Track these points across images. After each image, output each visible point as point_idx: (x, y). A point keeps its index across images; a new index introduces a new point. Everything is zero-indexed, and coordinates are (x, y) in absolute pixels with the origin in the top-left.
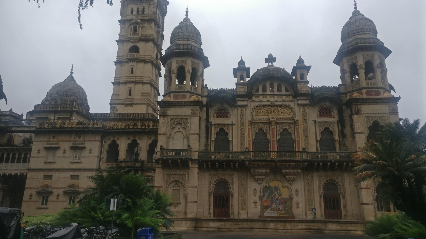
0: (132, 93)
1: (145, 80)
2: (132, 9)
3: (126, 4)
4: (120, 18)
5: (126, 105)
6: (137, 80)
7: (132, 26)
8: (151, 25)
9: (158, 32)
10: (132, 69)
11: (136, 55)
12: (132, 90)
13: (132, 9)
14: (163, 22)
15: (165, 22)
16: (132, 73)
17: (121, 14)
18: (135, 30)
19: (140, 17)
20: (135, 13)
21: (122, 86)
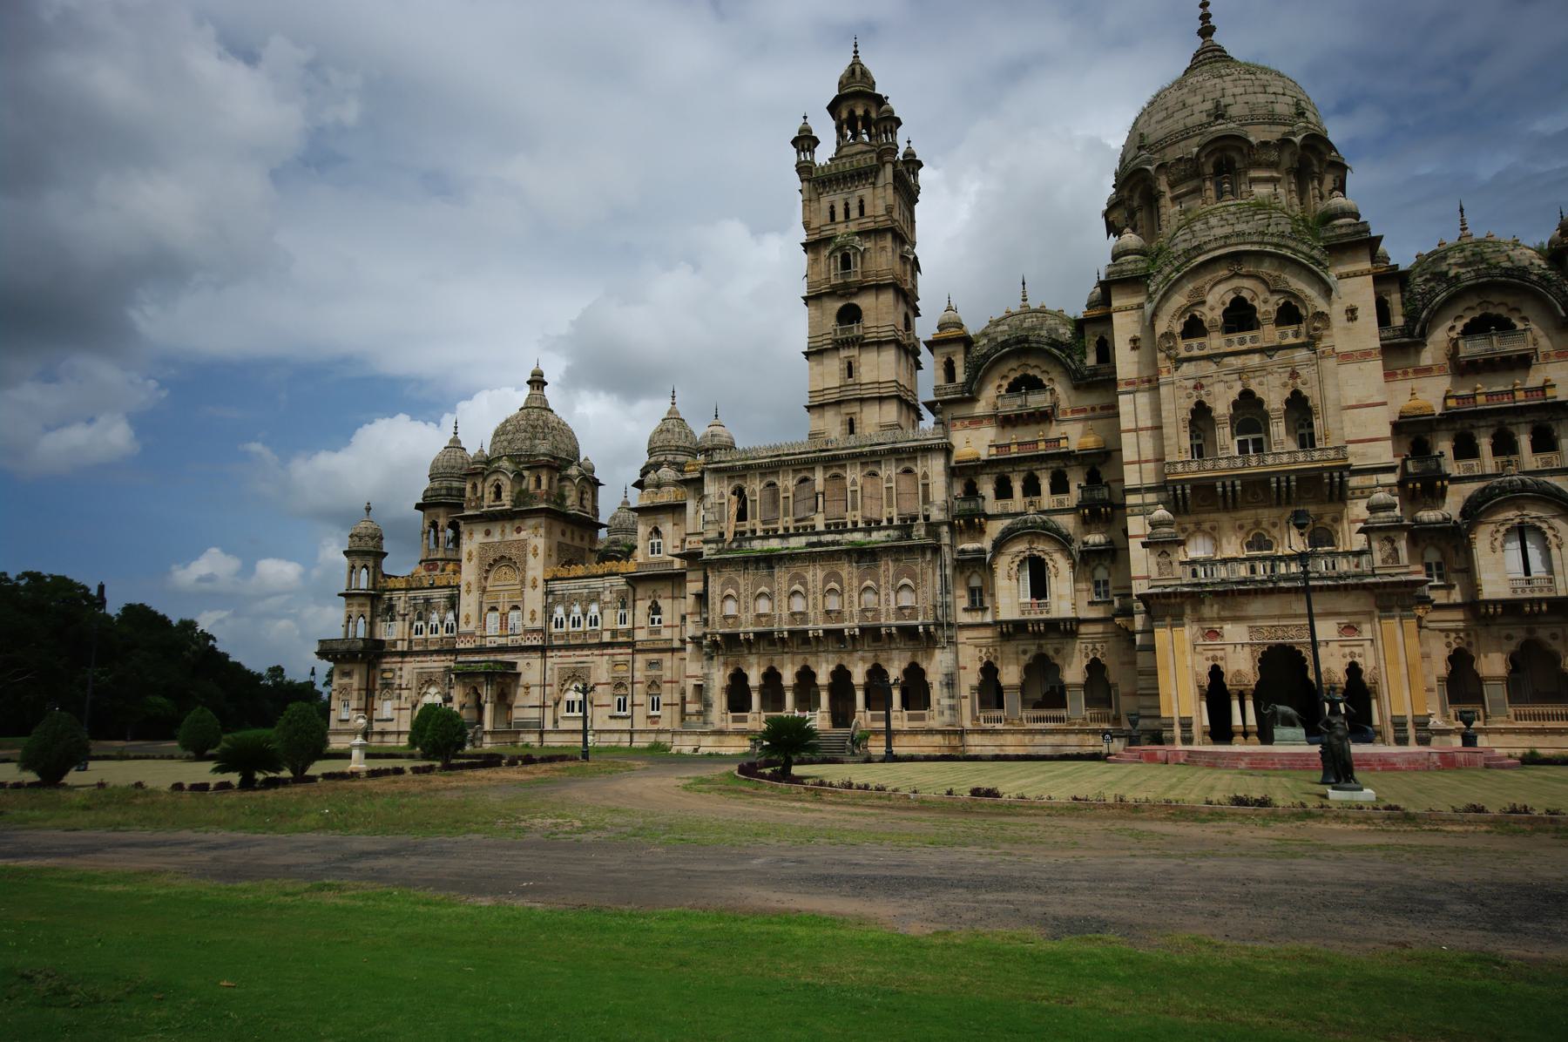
0: (857, 430)
1: (884, 392)
2: (832, 207)
3: (814, 196)
4: (803, 237)
6: (866, 394)
7: (839, 255)
8: (881, 244)
9: (904, 258)
10: (850, 364)
11: (857, 331)
12: (857, 418)
13: (832, 207)
14: (913, 222)
15: (917, 218)
16: (850, 376)
17: (806, 225)
18: (846, 263)
19: (853, 227)
20: (840, 216)
21: (830, 414)
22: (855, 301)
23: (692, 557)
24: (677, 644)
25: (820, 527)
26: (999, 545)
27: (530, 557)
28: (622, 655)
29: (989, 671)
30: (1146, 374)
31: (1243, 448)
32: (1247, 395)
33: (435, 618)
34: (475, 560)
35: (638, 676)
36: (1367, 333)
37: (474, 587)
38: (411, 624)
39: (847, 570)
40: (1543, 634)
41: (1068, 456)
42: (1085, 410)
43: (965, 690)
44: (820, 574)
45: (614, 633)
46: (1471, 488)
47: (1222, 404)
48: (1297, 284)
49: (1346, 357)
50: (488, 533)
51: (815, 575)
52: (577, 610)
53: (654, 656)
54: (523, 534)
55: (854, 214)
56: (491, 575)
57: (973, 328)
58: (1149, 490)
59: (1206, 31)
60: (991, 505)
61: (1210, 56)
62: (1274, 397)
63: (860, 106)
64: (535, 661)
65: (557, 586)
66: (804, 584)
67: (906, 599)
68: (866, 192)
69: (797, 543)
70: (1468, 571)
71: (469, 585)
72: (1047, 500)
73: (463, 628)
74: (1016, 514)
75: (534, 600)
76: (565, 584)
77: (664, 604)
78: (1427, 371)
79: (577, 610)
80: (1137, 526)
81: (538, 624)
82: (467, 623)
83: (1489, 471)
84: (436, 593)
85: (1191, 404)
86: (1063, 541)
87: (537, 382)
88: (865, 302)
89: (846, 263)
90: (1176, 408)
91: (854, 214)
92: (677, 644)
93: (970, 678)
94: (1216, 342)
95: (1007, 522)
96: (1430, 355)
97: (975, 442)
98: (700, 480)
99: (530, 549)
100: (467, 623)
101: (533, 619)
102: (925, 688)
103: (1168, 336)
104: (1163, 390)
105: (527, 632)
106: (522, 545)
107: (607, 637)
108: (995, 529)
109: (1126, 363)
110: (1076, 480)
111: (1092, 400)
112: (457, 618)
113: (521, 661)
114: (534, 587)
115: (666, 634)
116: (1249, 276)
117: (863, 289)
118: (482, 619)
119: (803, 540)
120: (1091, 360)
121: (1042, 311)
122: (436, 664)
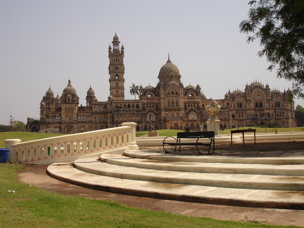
5: (117, 97)
7: (116, 67)
22: (118, 74)
23: (111, 112)
24: (99, 123)
25: (127, 110)
26: (148, 112)
27: (74, 110)
28: (90, 124)
29: (146, 126)
30: (164, 97)
31: (172, 106)
32: (173, 101)
33: (56, 118)
34: (64, 110)
35: (93, 127)
36: (182, 95)
37: (64, 114)
38: (52, 119)
39: (131, 115)
40: (193, 123)
41: (155, 104)
42: (156, 99)
43: (143, 128)
44: (128, 116)
45: (89, 121)
46: (189, 110)
47: (171, 101)
48: (178, 90)
49: (181, 98)
50: (66, 106)
51: (127, 116)
52: (82, 117)
53: (96, 124)
54: (73, 106)
55: (118, 61)
56: (67, 112)
57: (144, 87)
58: (164, 109)
59: (169, 58)
60: (146, 109)
61: (169, 61)
62: (175, 101)
63: (116, 41)
64: (76, 125)
65: (79, 114)
66: (126, 116)
67: (138, 118)
68: (119, 58)
69: (124, 111)
70: (188, 117)
71: (63, 113)
72: (152, 108)
73: (62, 120)
74: (149, 110)
75: (75, 116)
76: (80, 114)
77: (97, 117)
78: (186, 98)
79: (82, 117)
80: (162, 112)
81: (76, 119)
82: (63, 119)
83: (190, 108)
84: (57, 114)
85: (168, 101)
86: (154, 113)
87: (69, 82)
88: (119, 74)
89: (117, 68)
90: (167, 102)
91: (118, 61)
92: (99, 123)
93: (144, 127)
94: (170, 95)
95: (148, 110)
96: (186, 97)
97: (145, 101)
98: (112, 103)
99: (74, 109)
100: (63, 119)
101: (75, 119)
102: (139, 128)
103: (166, 94)
104: (166, 99)
105: (74, 121)
106: (73, 108)
107: (88, 121)
108: (147, 111)
109: (162, 96)
110: (155, 106)
111: (157, 98)
112: (61, 118)
113: (73, 125)
114: (75, 114)
115: (98, 121)
116: (174, 89)
117: (119, 73)
118: (66, 118)
119: (125, 111)
120: (157, 94)
121: (151, 87)
122: (58, 125)
